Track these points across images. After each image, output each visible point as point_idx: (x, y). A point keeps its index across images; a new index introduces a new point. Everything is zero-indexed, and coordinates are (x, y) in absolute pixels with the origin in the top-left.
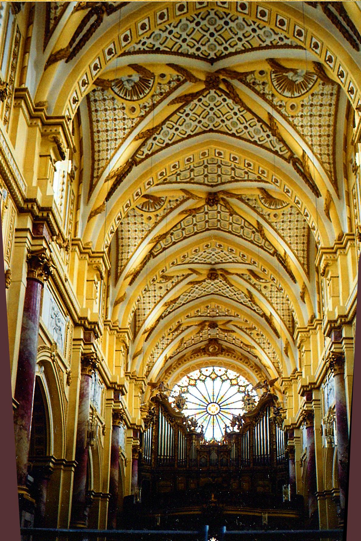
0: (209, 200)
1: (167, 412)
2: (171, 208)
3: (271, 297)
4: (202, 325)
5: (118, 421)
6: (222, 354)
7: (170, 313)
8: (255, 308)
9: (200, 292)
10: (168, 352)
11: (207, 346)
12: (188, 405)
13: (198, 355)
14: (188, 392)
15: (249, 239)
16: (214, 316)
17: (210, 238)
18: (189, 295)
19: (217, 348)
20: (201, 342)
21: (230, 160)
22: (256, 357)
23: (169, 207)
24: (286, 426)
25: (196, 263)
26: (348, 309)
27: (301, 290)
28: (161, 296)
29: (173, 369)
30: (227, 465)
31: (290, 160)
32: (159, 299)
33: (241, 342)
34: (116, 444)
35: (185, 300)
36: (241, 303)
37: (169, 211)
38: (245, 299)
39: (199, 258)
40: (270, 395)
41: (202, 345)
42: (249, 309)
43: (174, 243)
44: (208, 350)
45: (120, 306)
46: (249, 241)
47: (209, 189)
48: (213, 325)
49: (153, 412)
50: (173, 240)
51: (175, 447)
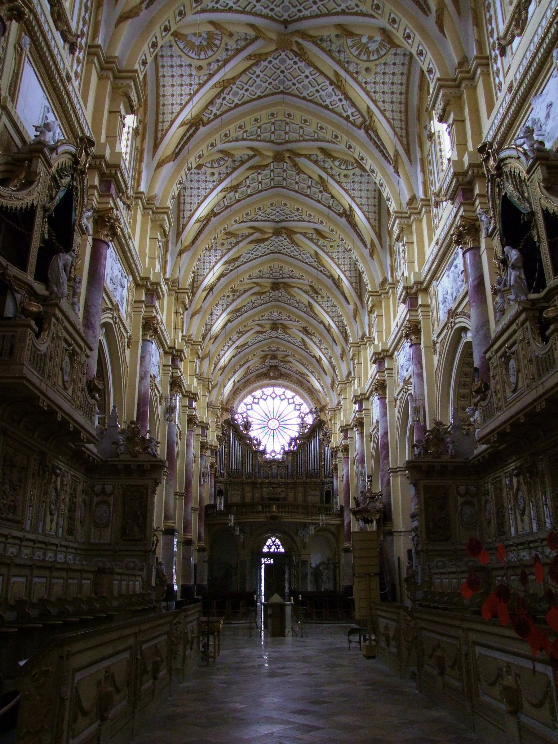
4: (264, 357)
5: (204, 451)
7: (239, 353)
10: (236, 377)
11: (269, 370)
12: (254, 427)
14: (252, 409)
17: (273, 307)
22: (309, 382)
30: (285, 478)
31: (361, 126)
40: (320, 420)
41: (264, 370)
43: (246, 312)
47: (274, 280)
48: (274, 357)
51: (243, 463)
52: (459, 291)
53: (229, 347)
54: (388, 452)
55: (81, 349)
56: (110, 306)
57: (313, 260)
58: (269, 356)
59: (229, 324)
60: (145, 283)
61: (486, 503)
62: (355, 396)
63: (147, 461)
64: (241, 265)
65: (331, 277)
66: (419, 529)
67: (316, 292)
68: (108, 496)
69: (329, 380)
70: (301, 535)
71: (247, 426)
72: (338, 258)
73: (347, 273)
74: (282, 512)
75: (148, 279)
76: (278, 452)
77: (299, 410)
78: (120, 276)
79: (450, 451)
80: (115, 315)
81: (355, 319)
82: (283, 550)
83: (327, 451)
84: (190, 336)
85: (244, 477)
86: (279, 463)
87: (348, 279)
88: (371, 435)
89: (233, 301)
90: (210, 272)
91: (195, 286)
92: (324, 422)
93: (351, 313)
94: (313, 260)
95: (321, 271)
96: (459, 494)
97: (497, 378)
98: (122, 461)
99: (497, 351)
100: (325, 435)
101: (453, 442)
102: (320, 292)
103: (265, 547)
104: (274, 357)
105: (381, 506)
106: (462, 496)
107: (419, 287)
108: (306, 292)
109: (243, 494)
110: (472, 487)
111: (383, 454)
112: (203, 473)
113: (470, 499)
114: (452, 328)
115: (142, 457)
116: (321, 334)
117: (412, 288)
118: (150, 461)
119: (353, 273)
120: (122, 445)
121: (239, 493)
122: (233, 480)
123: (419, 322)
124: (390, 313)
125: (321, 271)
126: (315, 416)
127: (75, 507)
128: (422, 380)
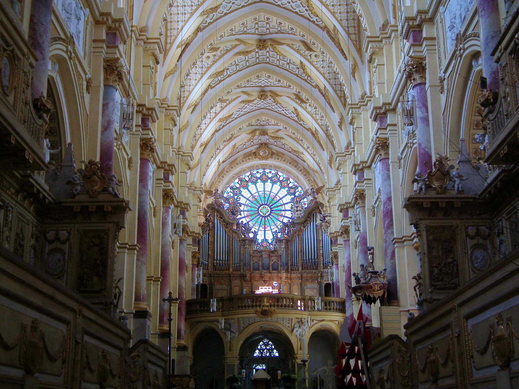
0: (260, 46)
1: (222, 218)
2: (227, 50)
3: (315, 114)
4: (253, 132)
6: (272, 158)
7: (224, 126)
8: (302, 123)
9: (252, 108)
10: (221, 157)
13: (249, 159)
15: (295, 73)
16: (263, 125)
18: (241, 110)
19: (267, 152)
20: (252, 146)
21: (277, 23)
22: (305, 162)
23: (225, 49)
24: (330, 233)
25: (248, 87)
26: (368, 156)
27: (338, 120)
28: (216, 113)
29: (225, 172)
32: (214, 115)
33: (290, 148)
34: (182, 256)
35: (237, 115)
36: (289, 117)
37: (225, 52)
38: (292, 114)
39: (250, 83)
40: (316, 202)
41: (253, 149)
42: (296, 123)
44: (259, 154)
45: (182, 134)
46: (294, 74)
49: (209, 218)
50: (229, 73)
52: (468, 10)
53: (211, 120)
54: (392, 220)
55: (24, 55)
56: (63, 36)
57: (304, 9)
58: (258, 133)
59: (210, 91)
60: (105, 19)
61: (501, 243)
62: (354, 165)
63: (108, 202)
64: (221, 17)
65: (325, 28)
66: (422, 276)
67: (309, 49)
68: (63, 243)
69: (325, 156)
70: (298, 333)
71: (234, 211)
72: (333, 6)
73: (344, 23)
74: (274, 306)
75: (108, 14)
76: (270, 241)
77: (294, 194)
78: (74, 5)
79: (456, 186)
80: (70, 48)
81: (354, 77)
82: (277, 355)
83: (327, 238)
84: (164, 100)
85: (231, 270)
86: (272, 252)
87: (345, 30)
88: (374, 208)
89: (214, 62)
90: (185, 24)
91: (168, 41)
92: (322, 205)
93: (348, 70)
94: (304, 9)
95: (313, 22)
96: (468, 235)
97: (506, 79)
98: (78, 202)
99: (506, 48)
100: (323, 219)
101: (460, 176)
102: (312, 47)
103: (257, 351)
104: (264, 133)
105: (385, 281)
106: (472, 238)
107: (423, 17)
108: (298, 51)
109: (231, 288)
110: (484, 228)
111: (387, 222)
112: (175, 225)
113: (481, 241)
114: (461, 56)
115: (102, 197)
116: (316, 101)
117: (414, 19)
118: (111, 202)
119: (351, 23)
120: (78, 184)
121: (225, 287)
122: (218, 272)
123: (424, 59)
124: (392, 60)
125: (313, 22)
126: (310, 198)
127: (23, 251)
128: (428, 125)
